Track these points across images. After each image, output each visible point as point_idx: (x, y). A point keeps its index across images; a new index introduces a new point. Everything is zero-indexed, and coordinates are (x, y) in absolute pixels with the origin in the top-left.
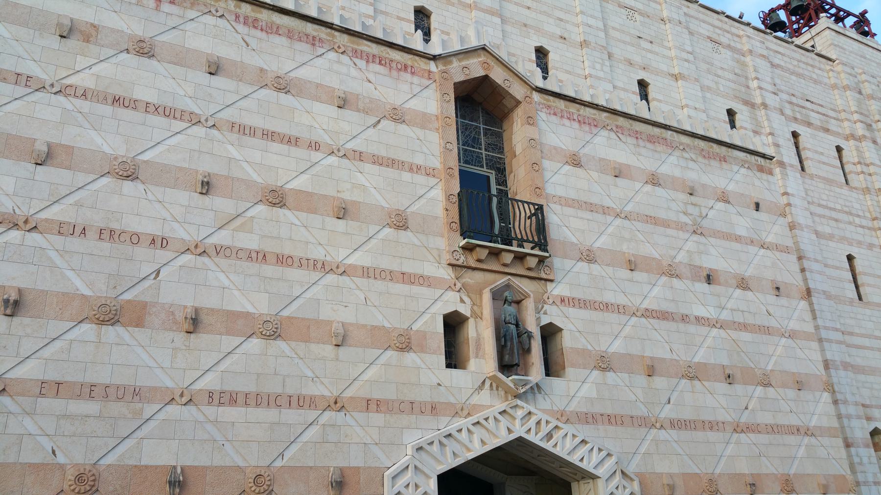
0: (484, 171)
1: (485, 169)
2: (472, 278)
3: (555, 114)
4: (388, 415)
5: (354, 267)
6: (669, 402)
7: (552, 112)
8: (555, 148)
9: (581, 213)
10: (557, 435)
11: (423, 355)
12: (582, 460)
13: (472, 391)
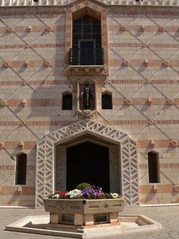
0: (91, 40)
1: (92, 39)
2: (74, 79)
3: (117, 13)
4: (39, 126)
5: (31, 82)
6: (159, 114)
7: (115, 13)
8: (116, 26)
9: (125, 48)
10: (104, 130)
11: (53, 107)
12: (113, 137)
13: (71, 117)
